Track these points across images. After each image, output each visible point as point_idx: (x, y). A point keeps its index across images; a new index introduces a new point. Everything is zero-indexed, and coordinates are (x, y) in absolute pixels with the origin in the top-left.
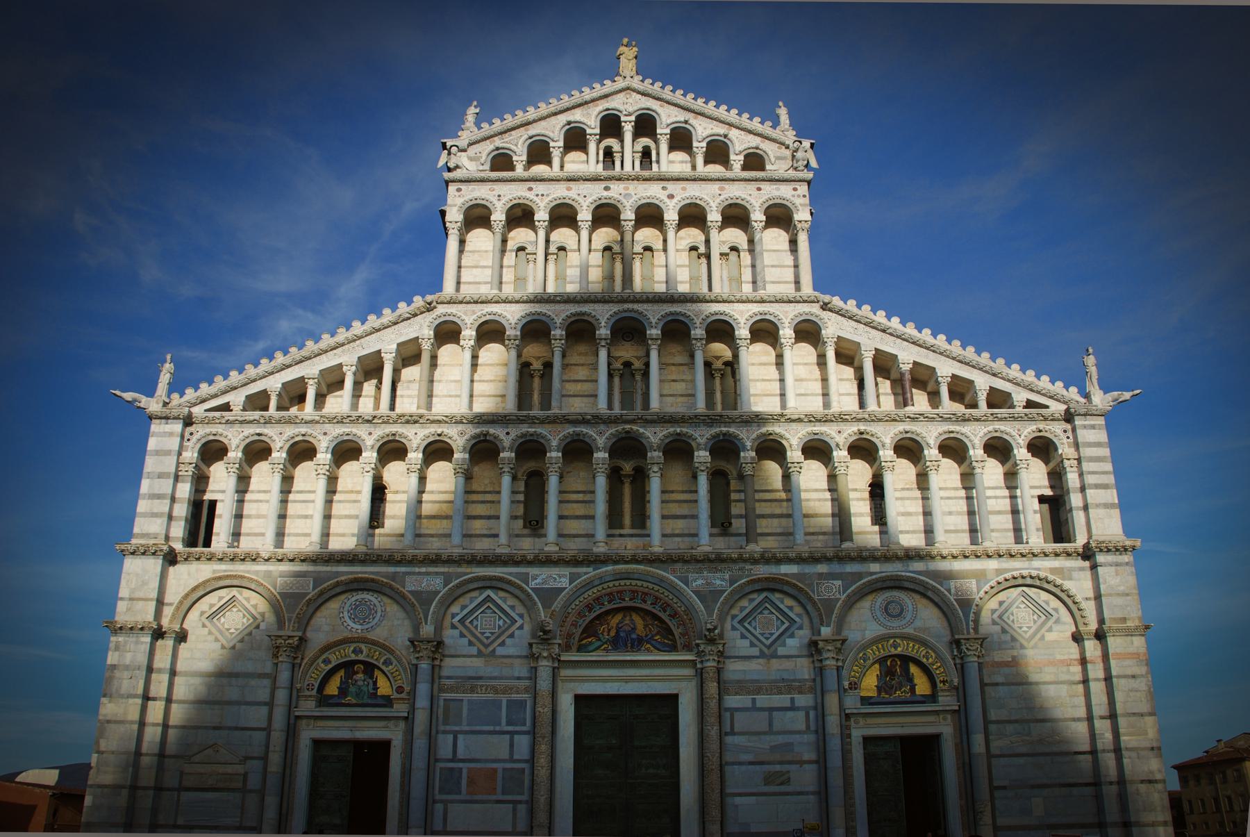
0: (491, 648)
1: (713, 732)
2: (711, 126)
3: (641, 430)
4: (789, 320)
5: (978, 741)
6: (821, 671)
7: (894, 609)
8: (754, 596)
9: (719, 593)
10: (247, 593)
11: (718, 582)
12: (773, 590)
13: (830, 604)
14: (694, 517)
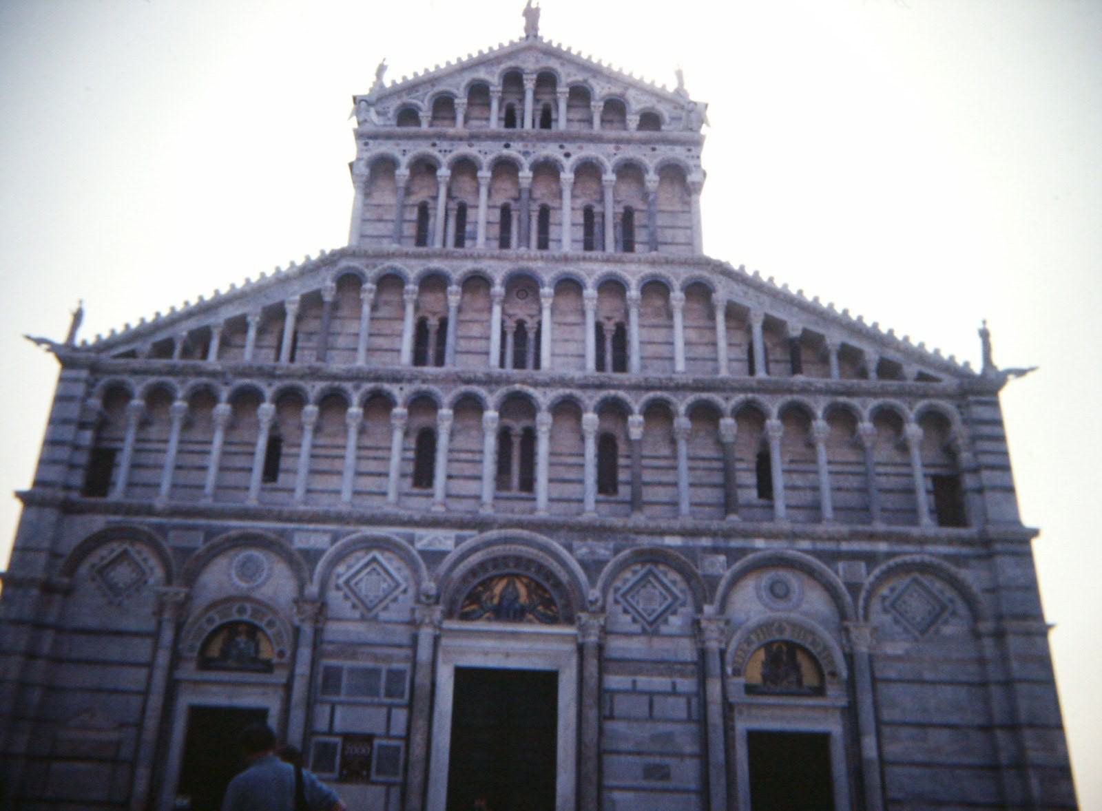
1: (592, 714)
2: (609, 85)
3: (531, 390)
4: (680, 282)
5: (869, 745)
6: (703, 653)
7: (779, 590)
8: (638, 567)
12: (656, 562)
13: (713, 581)
14: (581, 482)
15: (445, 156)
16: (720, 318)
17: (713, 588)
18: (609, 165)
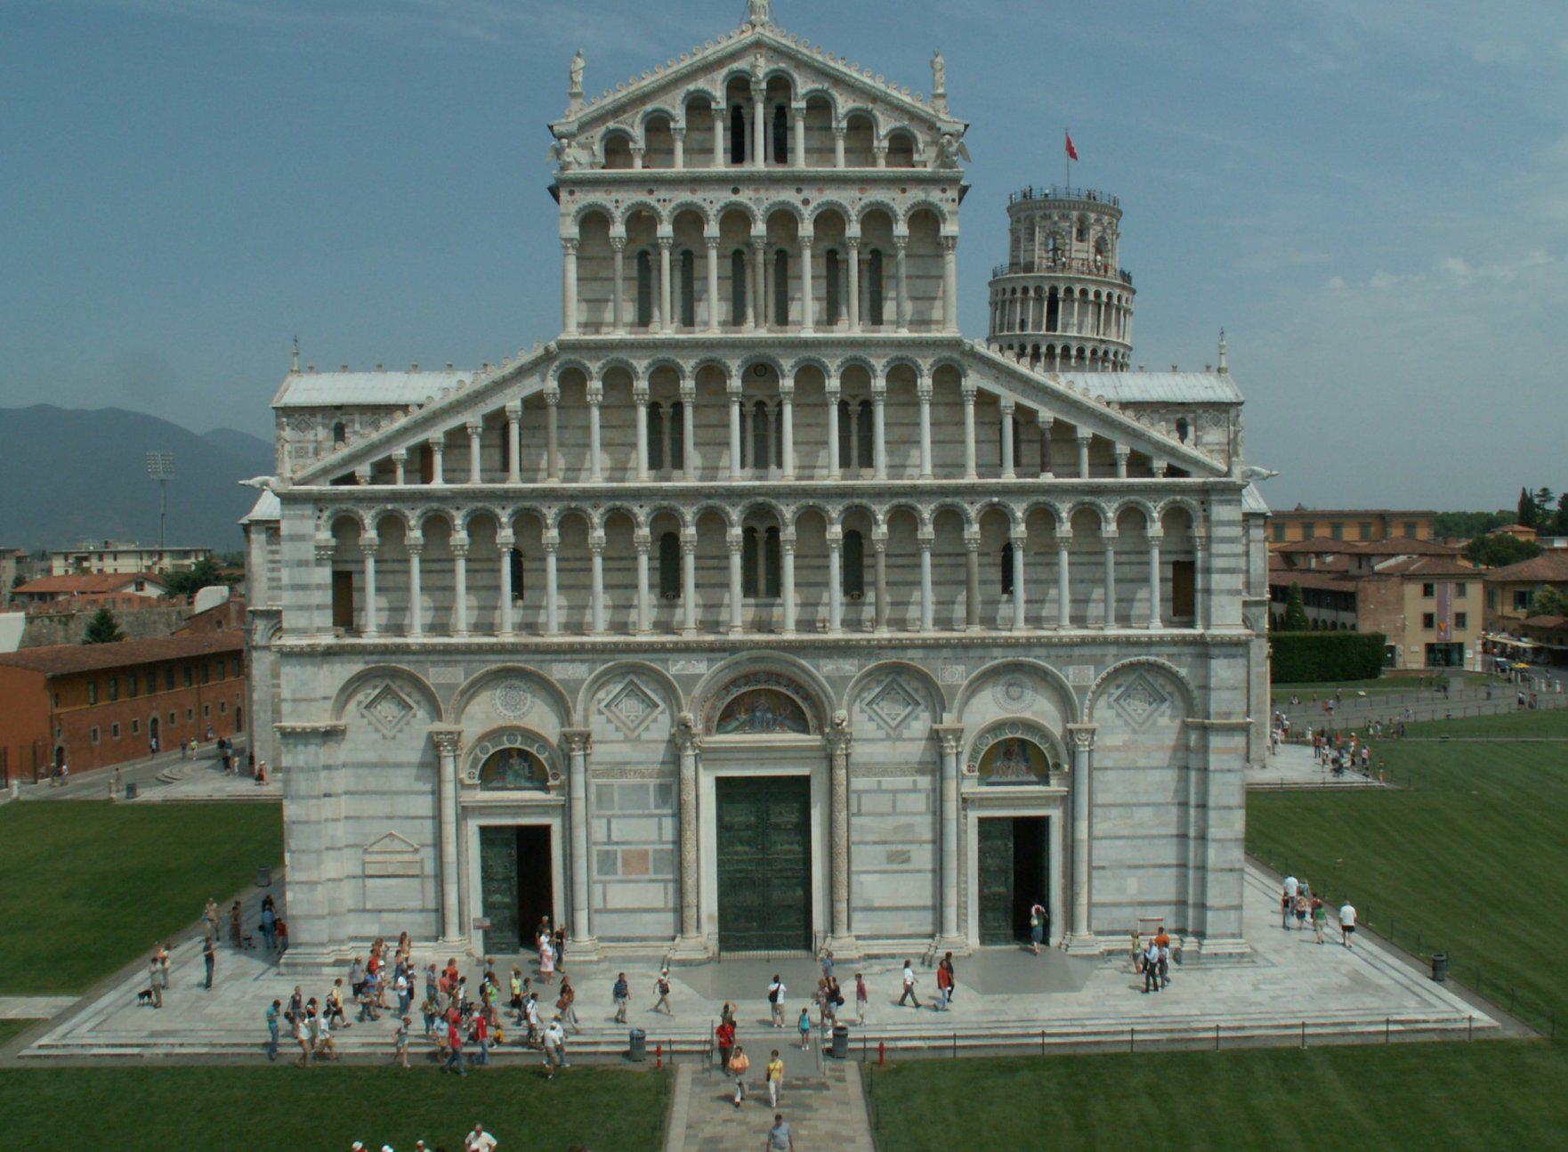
0: (636, 733)
3: (774, 502)
6: (942, 757)
9: (848, 678)
10: (399, 682)
11: (848, 667)
12: (899, 674)
13: (953, 689)
15: (664, 207)
16: (970, 409)
17: (953, 697)
18: (853, 213)
